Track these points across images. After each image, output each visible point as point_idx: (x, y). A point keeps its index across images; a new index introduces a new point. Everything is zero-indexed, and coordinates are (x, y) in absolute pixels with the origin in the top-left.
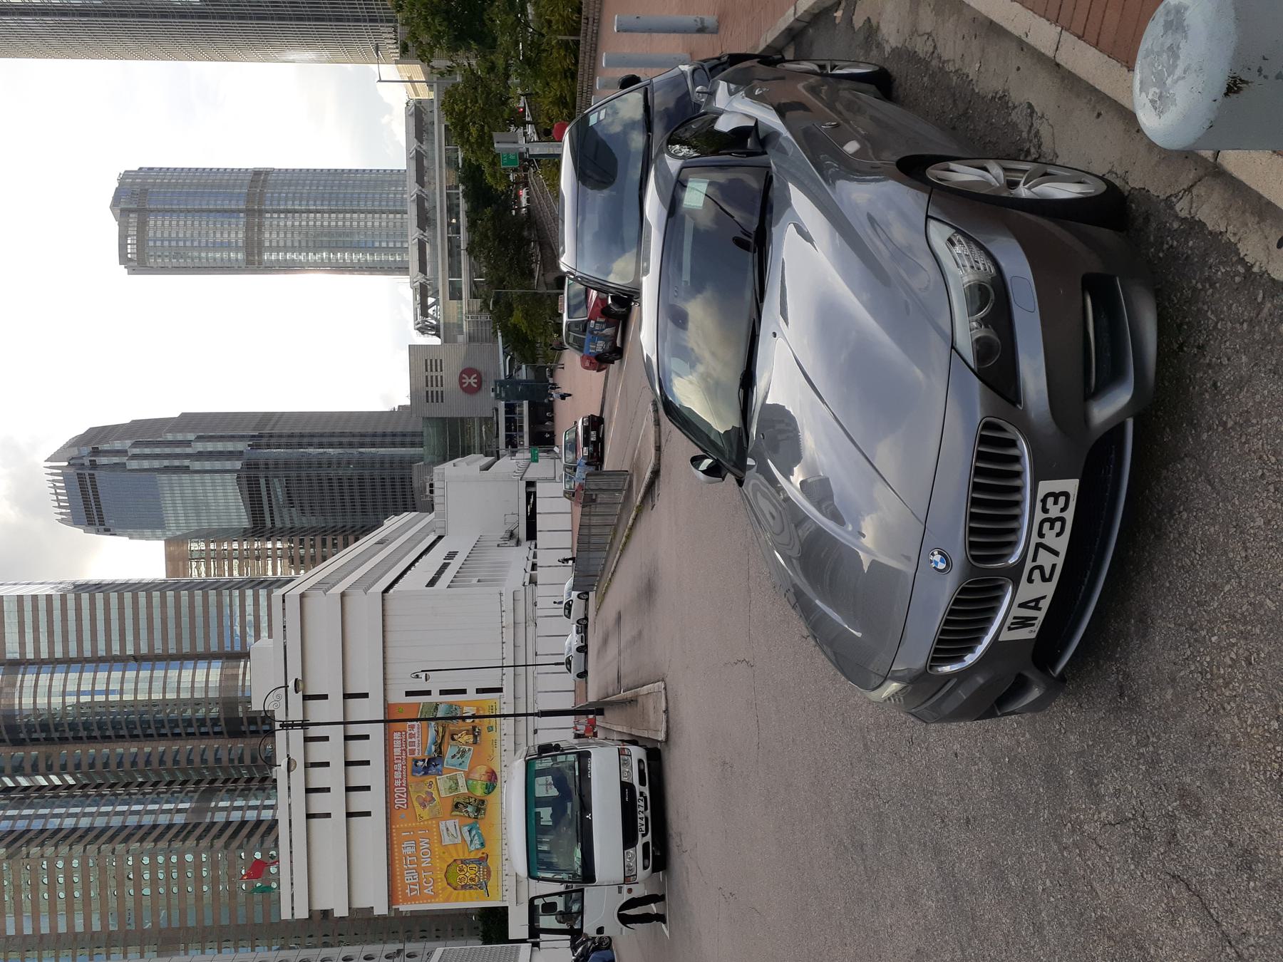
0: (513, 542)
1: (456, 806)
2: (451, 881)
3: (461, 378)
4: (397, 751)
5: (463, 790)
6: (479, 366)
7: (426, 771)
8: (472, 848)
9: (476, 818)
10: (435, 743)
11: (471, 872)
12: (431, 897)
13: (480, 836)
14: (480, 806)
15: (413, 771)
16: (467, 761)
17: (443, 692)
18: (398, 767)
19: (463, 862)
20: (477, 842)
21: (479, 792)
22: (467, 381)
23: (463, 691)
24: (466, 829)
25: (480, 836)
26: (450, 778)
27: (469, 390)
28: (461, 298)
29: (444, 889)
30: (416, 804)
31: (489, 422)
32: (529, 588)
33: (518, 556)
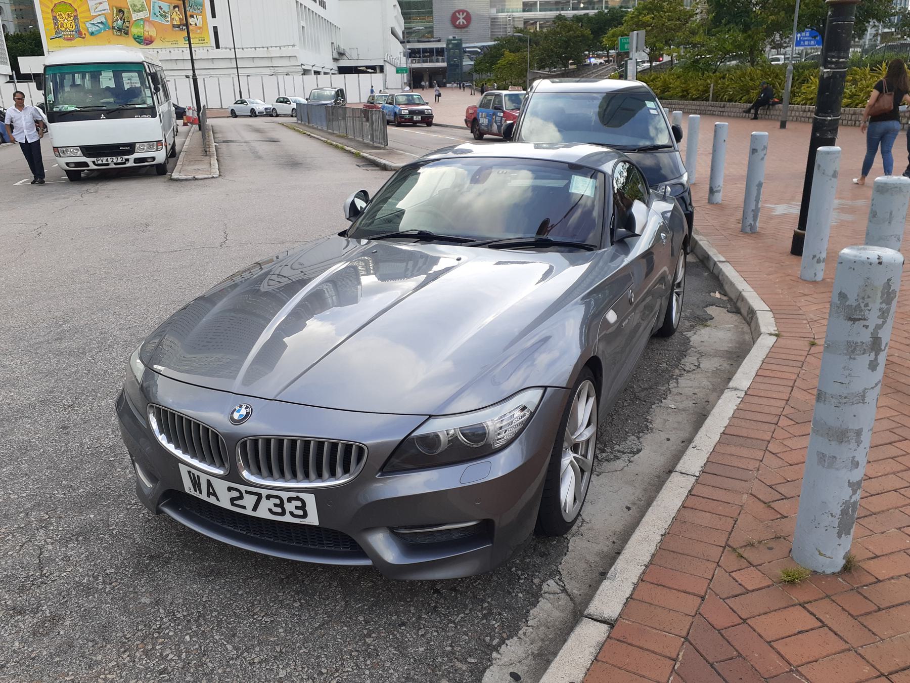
0: (336, 56)
1: (121, 11)
2: (59, 7)
3: (463, 11)
5: (135, 16)
6: (473, 25)
8: (88, 25)
11: (68, 23)
13: (99, 32)
14: (123, 31)
16: (159, 20)
19: (76, 18)
20: (94, 29)
21: (134, 30)
22: (461, 17)
23: (214, 16)
25: (99, 32)
26: (142, 6)
27: (454, 18)
28: (524, 11)
31: (429, 34)
32: (299, 69)
33: (325, 60)
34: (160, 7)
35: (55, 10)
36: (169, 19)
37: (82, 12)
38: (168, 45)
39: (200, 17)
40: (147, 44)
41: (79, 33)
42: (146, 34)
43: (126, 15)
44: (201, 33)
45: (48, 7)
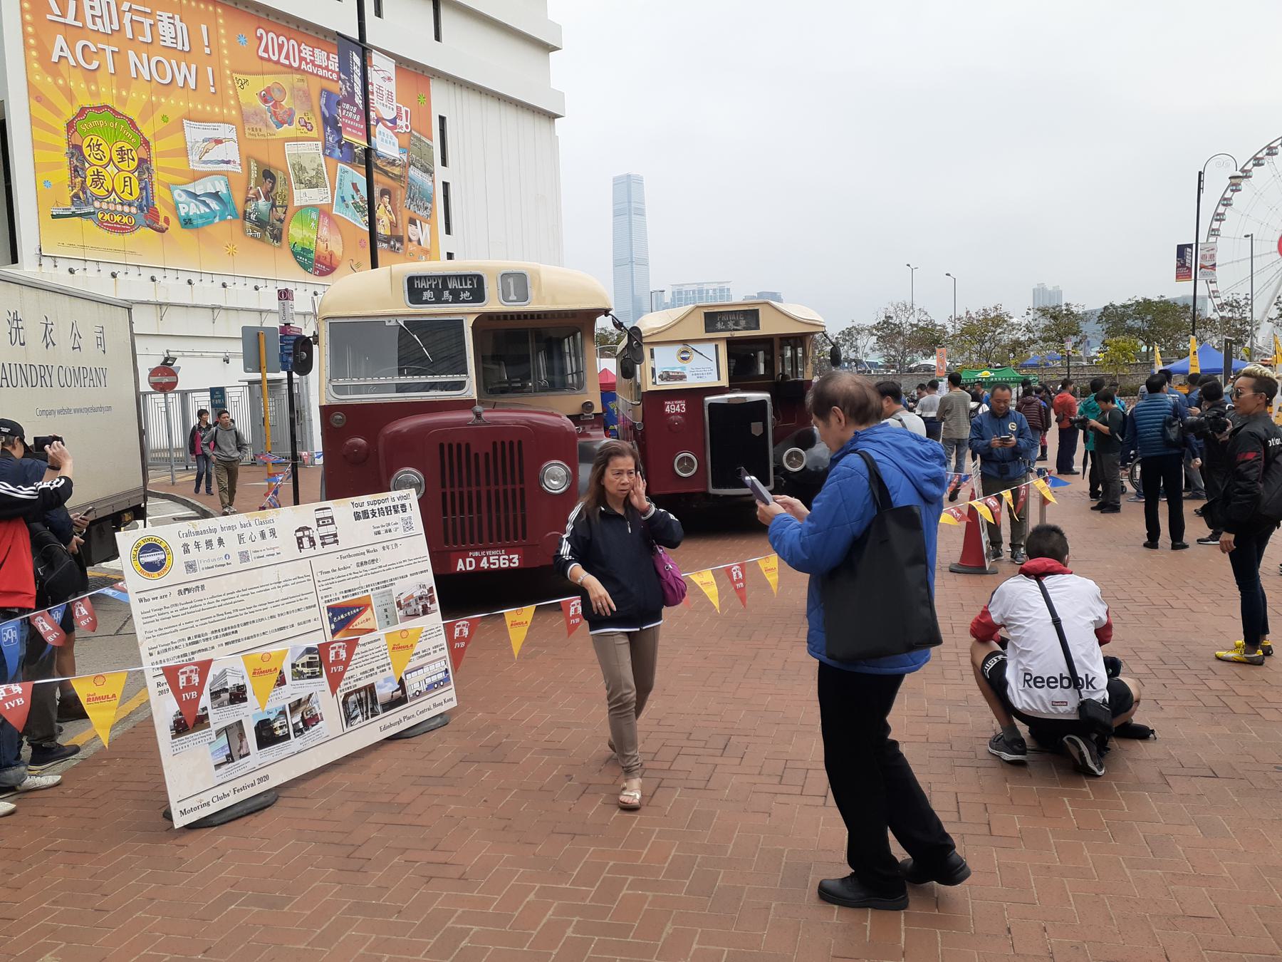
1: (268, 175)
2: (93, 119)
5: (301, 196)
9: (246, 216)
11: (118, 179)
13: (208, 219)
14: (268, 229)
17: (446, 185)
20: (191, 209)
21: (297, 232)
24: (221, 188)
25: (208, 219)
26: (319, 172)
30: (269, 81)
34: (354, 185)
35: (81, 126)
37: (162, 155)
39: (427, 227)
40: (322, 274)
41: (148, 214)
42: (322, 246)
43: (279, 188)
45: (58, 113)
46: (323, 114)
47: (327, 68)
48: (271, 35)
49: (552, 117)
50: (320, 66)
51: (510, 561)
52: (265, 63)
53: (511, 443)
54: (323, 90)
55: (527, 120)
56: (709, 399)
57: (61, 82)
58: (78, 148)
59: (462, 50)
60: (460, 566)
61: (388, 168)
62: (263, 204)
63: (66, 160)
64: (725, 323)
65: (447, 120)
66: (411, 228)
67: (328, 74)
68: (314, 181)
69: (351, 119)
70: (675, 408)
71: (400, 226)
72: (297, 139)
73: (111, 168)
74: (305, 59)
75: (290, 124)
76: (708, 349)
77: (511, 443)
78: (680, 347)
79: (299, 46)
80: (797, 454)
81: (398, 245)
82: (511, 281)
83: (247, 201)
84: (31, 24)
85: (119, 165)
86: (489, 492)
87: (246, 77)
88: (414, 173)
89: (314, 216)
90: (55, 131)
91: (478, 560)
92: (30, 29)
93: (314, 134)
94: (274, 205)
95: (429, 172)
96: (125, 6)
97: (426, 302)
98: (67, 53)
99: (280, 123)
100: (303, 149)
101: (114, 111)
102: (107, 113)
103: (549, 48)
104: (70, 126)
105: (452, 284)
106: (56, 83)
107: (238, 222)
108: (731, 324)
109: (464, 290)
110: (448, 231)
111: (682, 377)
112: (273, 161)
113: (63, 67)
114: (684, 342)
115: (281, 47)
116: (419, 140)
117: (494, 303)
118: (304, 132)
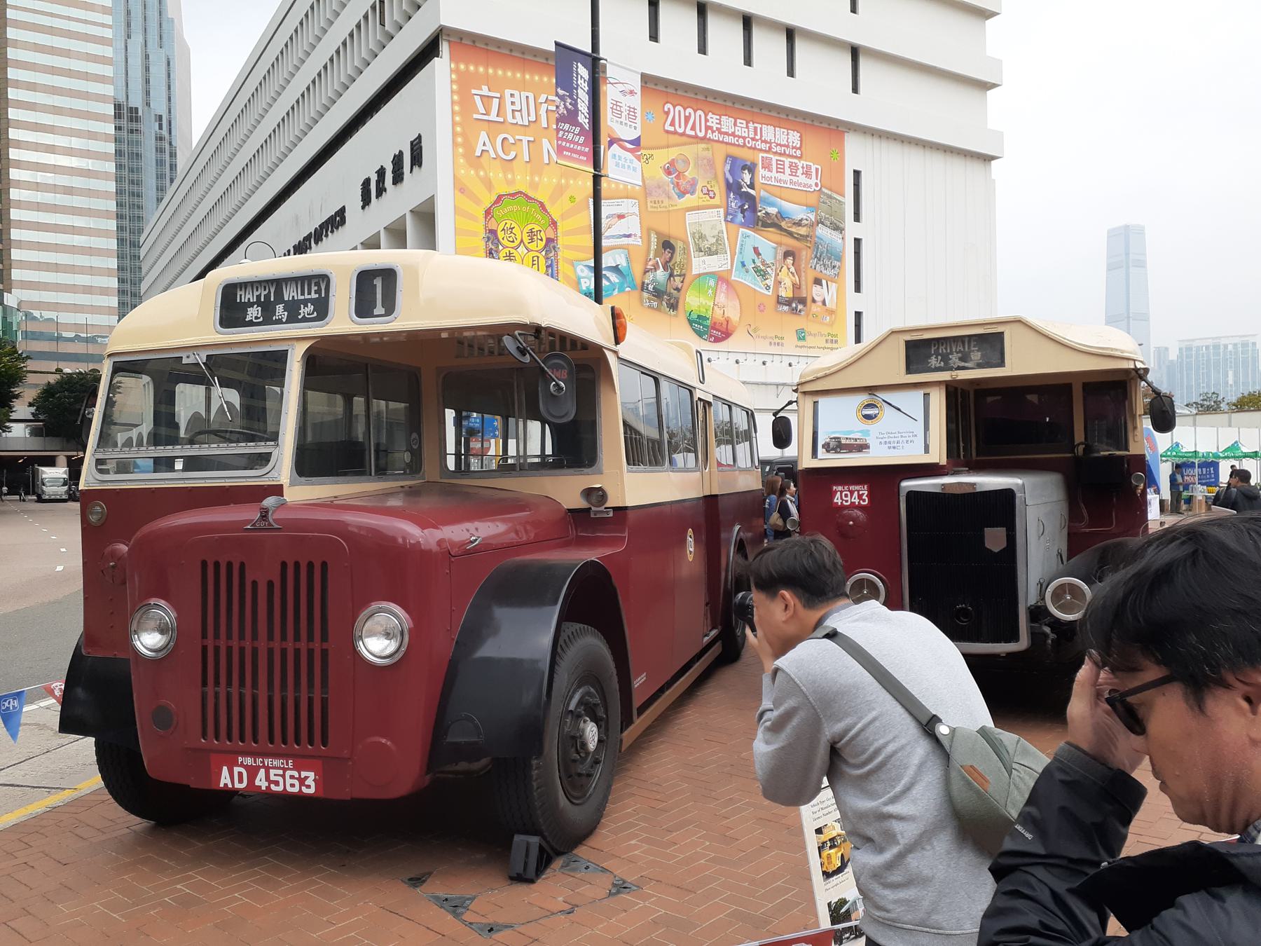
1: (667, 245)
2: (508, 205)
4: (769, 132)
5: (699, 264)
7: (733, 187)
9: (643, 287)
10: (781, 216)
12: (469, 146)
15: (734, 160)
16: (750, 280)
17: (858, 242)
18: (742, 128)
21: (693, 300)
24: (622, 262)
26: (719, 239)
29: (489, 185)
30: (673, 153)
34: (756, 250)
35: (497, 212)
36: (770, 282)
38: (763, 346)
39: (833, 287)
40: (717, 340)
42: (718, 312)
43: (678, 257)
44: (831, 324)
45: (477, 201)
46: (727, 181)
47: (733, 134)
48: (700, 112)
49: (987, 159)
50: (726, 133)
51: (302, 781)
52: (671, 136)
53: (310, 565)
54: (728, 156)
55: (958, 167)
56: (909, 484)
57: (482, 173)
58: (493, 232)
59: (885, 100)
60: (225, 780)
61: (793, 230)
62: (661, 274)
63: (483, 243)
64: (945, 358)
65: (863, 174)
66: (816, 290)
67: (734, 140)
68: (714, 249)
69: (571, 142)
70: (849, 497)
71: (803, 287)
72: (698, 208)
73: (522, 249)
74: (711, 128)
75: (693, 193)
76: (911, 401)
77: (310, 565)
78: (863, 398)
79: (706, 115)
80: (1073, 589)
81: (800, 307)
82: (378, 283)
83: (646, 272)
84: (460, 124)
85: (531, 246)
86: (270, 652)
87: (651, 152)
88: (823, 232)
89: (712, 283)
90: (473, 218)
91: (253, 771)
92: (458, 129)
93: (717, 201)
94: (671, 275)
95: (838, 228)
96: (542, 98)
97: (251, 324)
98: (489, 147)
99: (682, 194)
100: (706, 217)
101: (527, 196)
102: (521, 199)
103: (985, 86)
104: (488, 213)
105: (290, 293)
106: (477, 174)
107: (636, 294)
108: (954, 359)
109: (305, 302)
110: (858, 289)
111: (862, 447)
112: (673, 231)
113: (484, 160)
114: (871, 390)
115: (687, 119)
116: (830, 197)
117: (342, 320)
118: (706, 201)
